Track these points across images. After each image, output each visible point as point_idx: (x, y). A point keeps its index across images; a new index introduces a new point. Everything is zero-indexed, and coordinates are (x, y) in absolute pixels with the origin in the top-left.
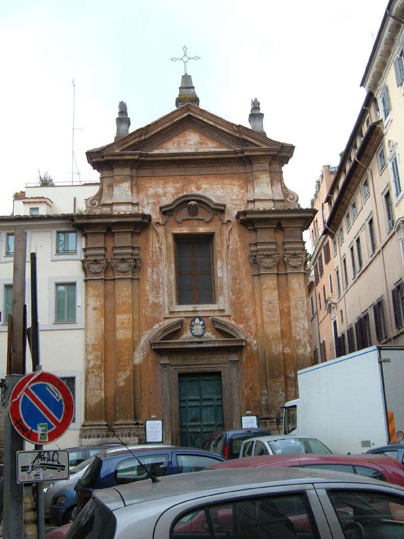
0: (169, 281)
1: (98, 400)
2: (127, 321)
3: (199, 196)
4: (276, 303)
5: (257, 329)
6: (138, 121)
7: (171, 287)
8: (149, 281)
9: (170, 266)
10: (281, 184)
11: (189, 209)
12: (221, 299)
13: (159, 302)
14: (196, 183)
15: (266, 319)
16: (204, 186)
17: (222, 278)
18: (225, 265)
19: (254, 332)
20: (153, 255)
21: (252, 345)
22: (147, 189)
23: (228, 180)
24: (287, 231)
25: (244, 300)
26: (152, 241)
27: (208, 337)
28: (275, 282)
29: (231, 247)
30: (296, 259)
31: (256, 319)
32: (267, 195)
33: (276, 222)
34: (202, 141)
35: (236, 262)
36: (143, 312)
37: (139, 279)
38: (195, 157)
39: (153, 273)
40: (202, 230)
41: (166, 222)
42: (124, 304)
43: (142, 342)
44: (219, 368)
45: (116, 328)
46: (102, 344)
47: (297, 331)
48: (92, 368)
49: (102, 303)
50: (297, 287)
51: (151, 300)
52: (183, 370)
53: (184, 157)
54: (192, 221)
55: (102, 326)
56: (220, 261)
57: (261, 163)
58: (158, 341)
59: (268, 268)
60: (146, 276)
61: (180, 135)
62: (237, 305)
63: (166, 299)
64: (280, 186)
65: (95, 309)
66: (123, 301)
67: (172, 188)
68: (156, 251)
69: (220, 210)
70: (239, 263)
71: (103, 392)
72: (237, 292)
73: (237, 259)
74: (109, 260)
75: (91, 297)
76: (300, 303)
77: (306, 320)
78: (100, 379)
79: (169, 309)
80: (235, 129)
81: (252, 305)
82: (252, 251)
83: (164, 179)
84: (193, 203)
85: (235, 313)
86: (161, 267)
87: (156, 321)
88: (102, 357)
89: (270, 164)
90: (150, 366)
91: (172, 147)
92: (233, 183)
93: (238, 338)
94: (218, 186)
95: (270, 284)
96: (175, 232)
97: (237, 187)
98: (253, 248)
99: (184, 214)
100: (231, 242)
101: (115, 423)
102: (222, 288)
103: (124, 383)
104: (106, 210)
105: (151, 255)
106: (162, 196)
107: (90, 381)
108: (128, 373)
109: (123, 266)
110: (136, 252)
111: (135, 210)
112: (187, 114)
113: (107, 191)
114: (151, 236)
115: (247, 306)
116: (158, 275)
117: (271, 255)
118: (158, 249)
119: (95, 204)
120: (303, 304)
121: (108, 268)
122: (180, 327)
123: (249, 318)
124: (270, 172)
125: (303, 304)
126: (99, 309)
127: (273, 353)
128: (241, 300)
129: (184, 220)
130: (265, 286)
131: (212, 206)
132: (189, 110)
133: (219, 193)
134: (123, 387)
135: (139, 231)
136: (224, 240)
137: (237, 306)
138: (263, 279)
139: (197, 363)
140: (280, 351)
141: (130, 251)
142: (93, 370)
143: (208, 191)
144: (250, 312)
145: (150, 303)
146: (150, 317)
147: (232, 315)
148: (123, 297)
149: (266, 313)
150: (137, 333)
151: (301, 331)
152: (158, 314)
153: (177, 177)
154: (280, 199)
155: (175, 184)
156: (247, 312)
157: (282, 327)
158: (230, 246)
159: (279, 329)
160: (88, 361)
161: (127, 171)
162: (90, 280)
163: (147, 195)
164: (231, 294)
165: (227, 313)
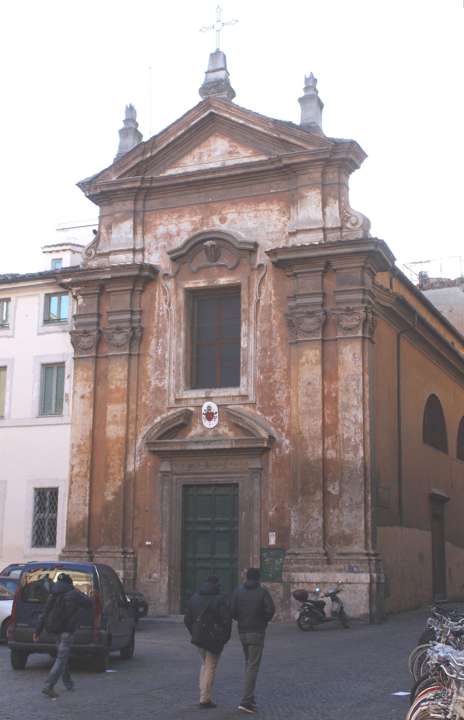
0: (178, 357)
1: (81, 518)
2: (120, 413)
3: (219, 232)
5: (290, 424)
6: (149, 130)
8: (152, 357)
10: (340, 202)
11: (206, 252)
12: (243, 380)
13: (164, 386)
14: (220, 213)
16: (230, 217)
18: (252, 331)
19: (286, 427)
20: (158, 320)
21: (283, 446)
22: (156, 227)
23: (264, 204)
25: (275, 381)
26: (159, 300)
27: (224, 434)
28: (318, 352)
29: (262, 303)
30: (352, 317)
32: (315, 222)
33: (323, 263)
34: (232, 149)
35: (269, 325)
36: (143, 400)
38: (216, 175)
39: (157, 345)
40: (223, 281)
42: (118, 389)
43: (140, 440)
45: (107, 422)
46: (89, 444)
47: (345, 425)
48: (77, 475)
49: (92, 389)
50: (350, 359)
51: (153, 383)
53: (202, 177)
55: (90, 420)
56: (245, 324)
57: (310, 173)
58: (153, 440)
59: (310, 332)
61: (203, 145)
63: (173, 382)
64: (337, 205)
65: (83, 397)
66: (116, 386)
67: (188, 223)
68: (163, 315)
71: (87, 508)
72: (267, 370)
73: (270, 321)
76: (354, 383)
77: (360, 410)
78: (84, 490)
80: (271, 126)
82: (291, 308)
83: (177, 212)
84: (208, 243)
85: (262, 400)
87: (158, 412)
88: (88, 461)
91: (190, 164)
92: (271, 207)
95: (311, 356)
96: (187, 286)
98: (292, 304)
99: (202, 259)
100: (263, 295)
101: (98, 550)
102: (246, 364)
103: (113, 497)
104: (103, 261)
105: (156, 321)
106: (174, 236)
107: (72, 493)
108: (119, 483)
109: (119, 338)
110: (137, 317)
111: (139, 258)
112: (208, 112)
113: (105, 235)
114: (157, 293)
115: (279, 389)
116: (164, 349)
117: (314, 312)
118: (165, 312)
119: (91, 254)
120: (358, 386)
121: (99, 342)
124: (323, 185)
125: (358, 386)
128: (272, 381)
129: (199, 269)
130: (303, 360)
132: (210, 106)
133: (250, 224)
134: (110, 502)
135: (141, 288)
136: (253, 292)
139: (207, 471)
140: (318, 455)
141: (128, 316)
142: (78, 479)
143: (236, 223)
144: (284, 398)
145: (151, 387)
146: (151, 407)
150: (133, 430)
151: (352, 426)
153: (195, 207)
154: (335, 226)
155: (192, 217)
156: (279, 398)
157: (326, 419)
158: (261, 302)
160: (72, 467)
161: (129, 205)
163: (155, 237)
164: (258, 372)
165: (251, 399)
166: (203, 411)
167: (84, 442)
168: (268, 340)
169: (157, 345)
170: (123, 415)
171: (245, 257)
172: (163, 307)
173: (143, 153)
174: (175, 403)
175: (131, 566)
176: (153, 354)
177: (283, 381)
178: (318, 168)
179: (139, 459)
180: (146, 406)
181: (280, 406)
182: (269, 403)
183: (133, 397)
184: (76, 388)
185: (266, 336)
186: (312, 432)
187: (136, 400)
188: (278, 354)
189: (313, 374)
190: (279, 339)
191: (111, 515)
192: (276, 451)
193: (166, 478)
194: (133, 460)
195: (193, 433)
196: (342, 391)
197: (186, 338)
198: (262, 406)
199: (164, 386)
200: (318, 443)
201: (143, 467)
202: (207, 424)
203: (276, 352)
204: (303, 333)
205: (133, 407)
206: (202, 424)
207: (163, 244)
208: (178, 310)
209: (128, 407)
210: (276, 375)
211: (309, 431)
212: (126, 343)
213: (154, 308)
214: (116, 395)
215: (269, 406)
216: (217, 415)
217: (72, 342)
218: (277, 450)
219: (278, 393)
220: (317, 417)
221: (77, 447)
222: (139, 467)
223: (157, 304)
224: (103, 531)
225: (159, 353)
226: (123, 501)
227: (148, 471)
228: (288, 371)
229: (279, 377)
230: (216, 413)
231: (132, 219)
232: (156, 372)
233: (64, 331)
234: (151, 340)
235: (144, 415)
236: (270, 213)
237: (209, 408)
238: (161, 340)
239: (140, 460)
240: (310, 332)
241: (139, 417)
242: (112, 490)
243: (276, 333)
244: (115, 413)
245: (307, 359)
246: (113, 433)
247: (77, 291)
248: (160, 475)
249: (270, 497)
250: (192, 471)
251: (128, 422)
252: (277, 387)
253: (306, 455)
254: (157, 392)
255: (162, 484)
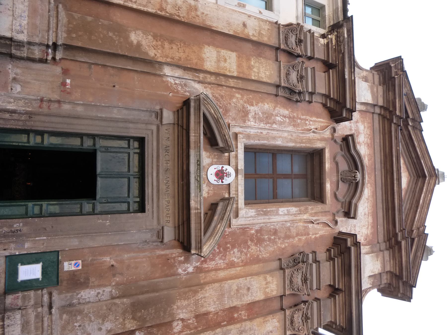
0: (274, 138)
2: (228, 67)
4: (248, 299)
5: (209, 271)
7: (267, 139)
8: (274, 109)
9: (291, 140)
10: (370, 288)
13: (249, 120)
15: (226, 285)
17: (277, 214)
18: (291, 218)
19: (205, 266)
21: (186, 265)
22: (363, 122)
24: (330, 302)
25: (249, 247)
26: (317, 121)
29: (310, 225)
31: (223, 269)
35: (295, 234)
37: (276, 95)
38: (395, 182)
39: (283, 116)
40: (328, 187)
41: (335, 141)
42: (250, 68)
44: (151, 210)
45: (219, 50)
46: (197, 22)
49: (251, 37)
50: (268, 329)
51: (252, 108)
52: (150, 150)
54: (335, 174)
58: (202, 108)
59: (291, 282)
60: (279, 106)
62: (242, 237)
63: (252, 131)
65: (244, 25)
69: (349, 213)
70: (293, 238)
73: (297, 235)
74: (300, 59)
75: (259, 23)
78: (144, 3)
79: (240, 133)
81: (242, 261)
83: (371, 144)
85: (233, 234)
86: (290, 128)
88: (179, 16)
89: (390, 272)
90: (160, 93)
92: (370, 227)
93: (203, 240)
94: (367, 209)
95: (272, 286)
97: (366, 233)
99: (344, 166)
101: (60, 6)
103: (135, 42)
105: (302, 117)
108: (152, 53)
109: (294, 76)
113: (362, 75)
114: (322, 120)
115: (242, 252)
116: (281, 123)
122: (221, 144)
123: (225, 257)
126: (244, 30)
127: (174, 303)
128: (249, 243)
129: (337, 164)
130: (269, 279)
131: (354, 201)
132: (431, 176)
136: (318, 216)
137: (243, 238)
138: (279, 274)
139: (161, 171)
140: (179, 314)
144: (234, 259)
145: (248, 106)
146: (230, 104)
147: (230, 230)
148: (259, 69)
149: (234, 284)
150: (209, 80)
152: (234, 115)
156: (234, 253)
159: (212, 309)
162: (279, 28)
164: (257, 227)
166: (226, 167)
167: (200, 16)
168: (282, 235)
169: (283, 116)
170: (226, 70)
171: (342, 207)
172: (312, 125)
173: (413, 120)
174: (233, 133)
175: (33, 54)
176: (276, 111)
177: (249, 255)
178: (393, 268)
179: (177, 82)
180: (232, 97)
181: (226, 255)
182: (229, 243)
183: (240, 84)
184: (253, 19)
185: (286, 232)
186: (202, 301)
187: (238, 86)
188: (271, 247)
189: (257, 292)
190: (283, 246)
191: (111, 34)
192: (181, 257)
193: (154, 116)
194: (176, 75)
195: (204, 154)
196: (241, 327)
197: (287, 147)
198: (227, 235)
199: (249, 120)
200: (192, 312)
201: (168, 87)
202: (212, 171)
203: (273, 245)
204: (290, 274)
205: (232, 83)
206: (212, 164)
207: (353, 129)
208: (310, 140)
209: (232, 77)
210: (254, 247)
211: (204, 297)
212: (290, 84)
213: (311, 117)
214: (244, 64)
215: (227, 243)
216: (220, 183)
217: (291, 24)
218: (182, 258)
219: (238, 252)
220: (218, 304)
221: (195, 6)
222: (168, 81)
223: (314, 119)
224: (89, 19)
225: (277, 118)
226: (130, 55)
227: (163, 93)
228: (256, 260)
229: (252, 251)
230: (222, 182)
231: (372, 103)
232: (262, 113)
233: (297, 17)
234: (287, 110)
235: (222, 94)
236: (366, 226)
237: (229, 175)
238: (287, 120)
239: (175, 84)
240: (291, 282)
241: (221, 88)
242: (144, 43)
243: (288, 243)
244: (228, 61)
245: (269, 282)
246: (208, 55)
247: (332, 39)
248: (158, 108)
249: (129, 255)
250: (161, 151)
251: (217, 75)
252: (244, 250)
253: (178, 299)
254: (243, 112)
255: (147, 111)
